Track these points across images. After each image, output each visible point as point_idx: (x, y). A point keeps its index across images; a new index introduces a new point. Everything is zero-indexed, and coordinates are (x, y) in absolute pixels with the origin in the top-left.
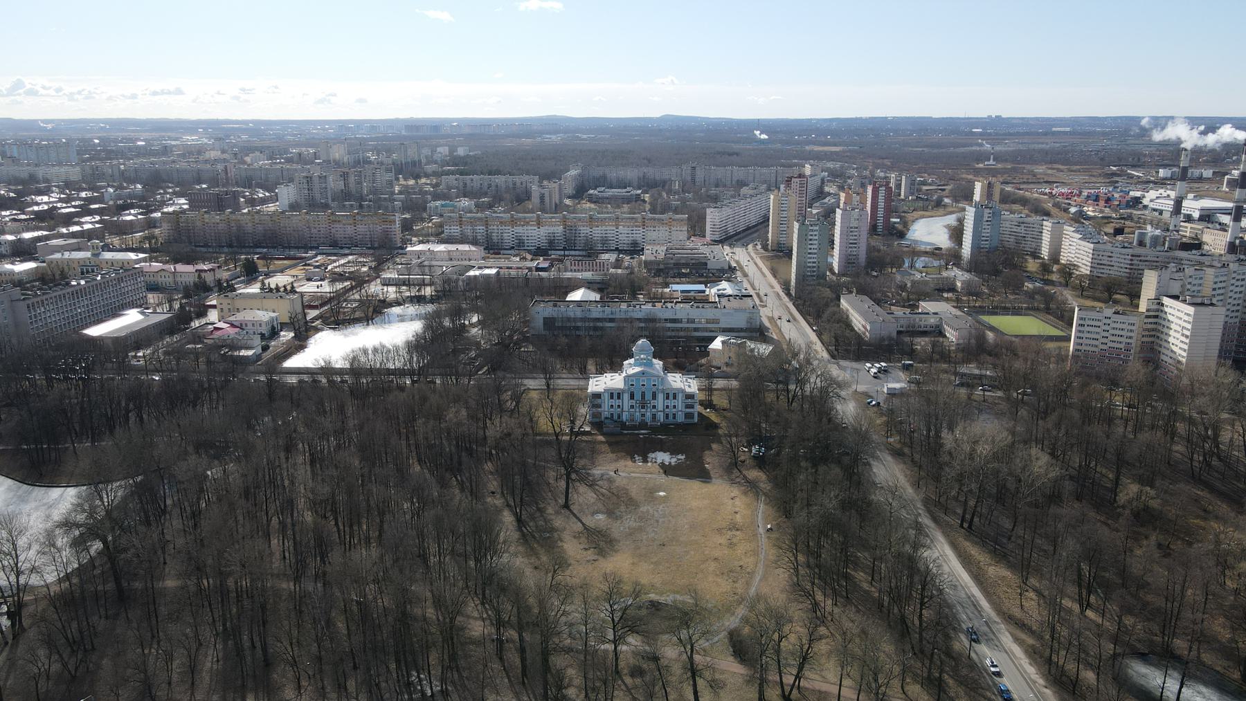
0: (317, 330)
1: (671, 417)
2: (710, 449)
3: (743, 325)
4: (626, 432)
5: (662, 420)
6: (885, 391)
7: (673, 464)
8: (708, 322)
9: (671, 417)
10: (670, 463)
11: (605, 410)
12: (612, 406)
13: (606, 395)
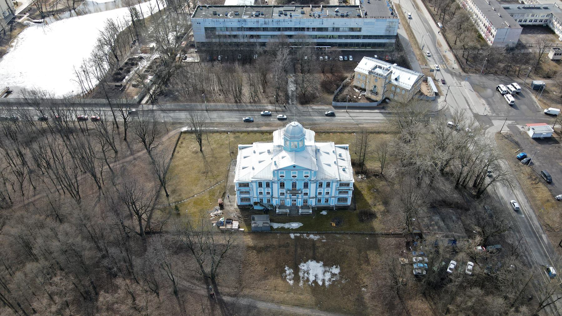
0: (23, 26)
1: (323, 201)
2: (367, 261)
3: (382, 33)
4: (276, 226)
5: (314, 204)
6: (531, 134)
7: (327, 283)
8: (352, 29)
9: (323, 201)
10: (324, 281)
11: (254, 196)
12: (261, 193)
13: (254, 184)
